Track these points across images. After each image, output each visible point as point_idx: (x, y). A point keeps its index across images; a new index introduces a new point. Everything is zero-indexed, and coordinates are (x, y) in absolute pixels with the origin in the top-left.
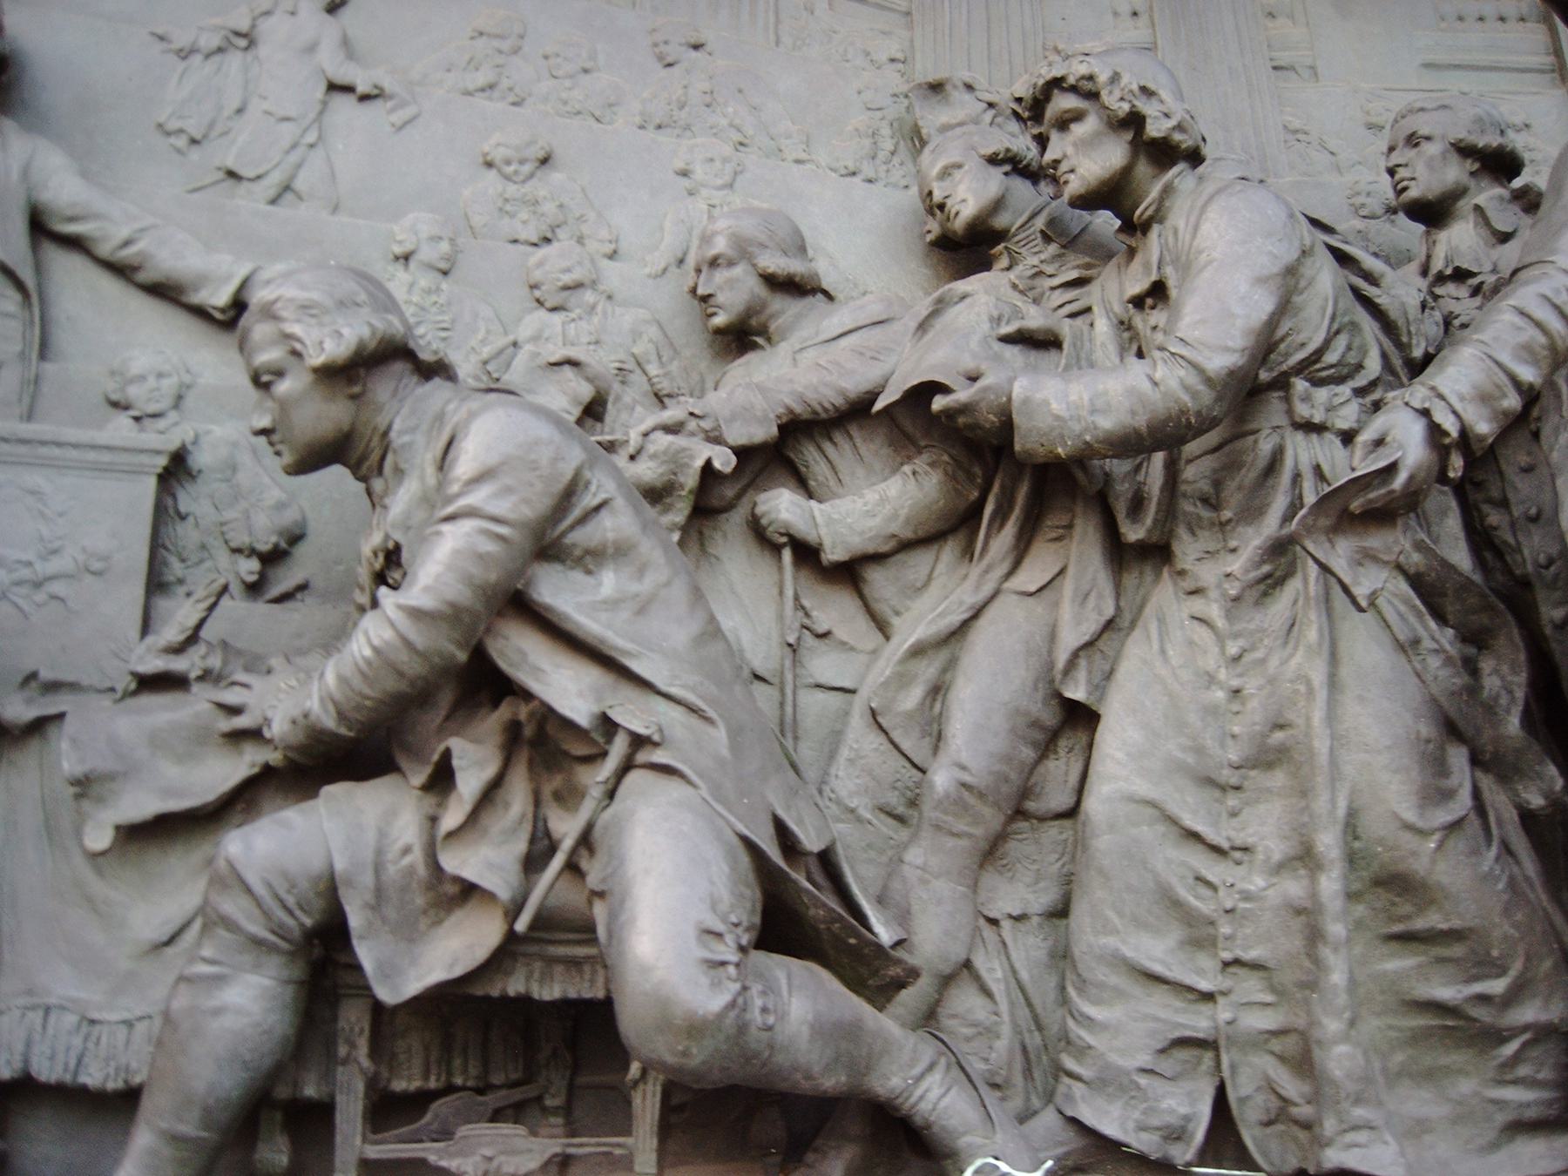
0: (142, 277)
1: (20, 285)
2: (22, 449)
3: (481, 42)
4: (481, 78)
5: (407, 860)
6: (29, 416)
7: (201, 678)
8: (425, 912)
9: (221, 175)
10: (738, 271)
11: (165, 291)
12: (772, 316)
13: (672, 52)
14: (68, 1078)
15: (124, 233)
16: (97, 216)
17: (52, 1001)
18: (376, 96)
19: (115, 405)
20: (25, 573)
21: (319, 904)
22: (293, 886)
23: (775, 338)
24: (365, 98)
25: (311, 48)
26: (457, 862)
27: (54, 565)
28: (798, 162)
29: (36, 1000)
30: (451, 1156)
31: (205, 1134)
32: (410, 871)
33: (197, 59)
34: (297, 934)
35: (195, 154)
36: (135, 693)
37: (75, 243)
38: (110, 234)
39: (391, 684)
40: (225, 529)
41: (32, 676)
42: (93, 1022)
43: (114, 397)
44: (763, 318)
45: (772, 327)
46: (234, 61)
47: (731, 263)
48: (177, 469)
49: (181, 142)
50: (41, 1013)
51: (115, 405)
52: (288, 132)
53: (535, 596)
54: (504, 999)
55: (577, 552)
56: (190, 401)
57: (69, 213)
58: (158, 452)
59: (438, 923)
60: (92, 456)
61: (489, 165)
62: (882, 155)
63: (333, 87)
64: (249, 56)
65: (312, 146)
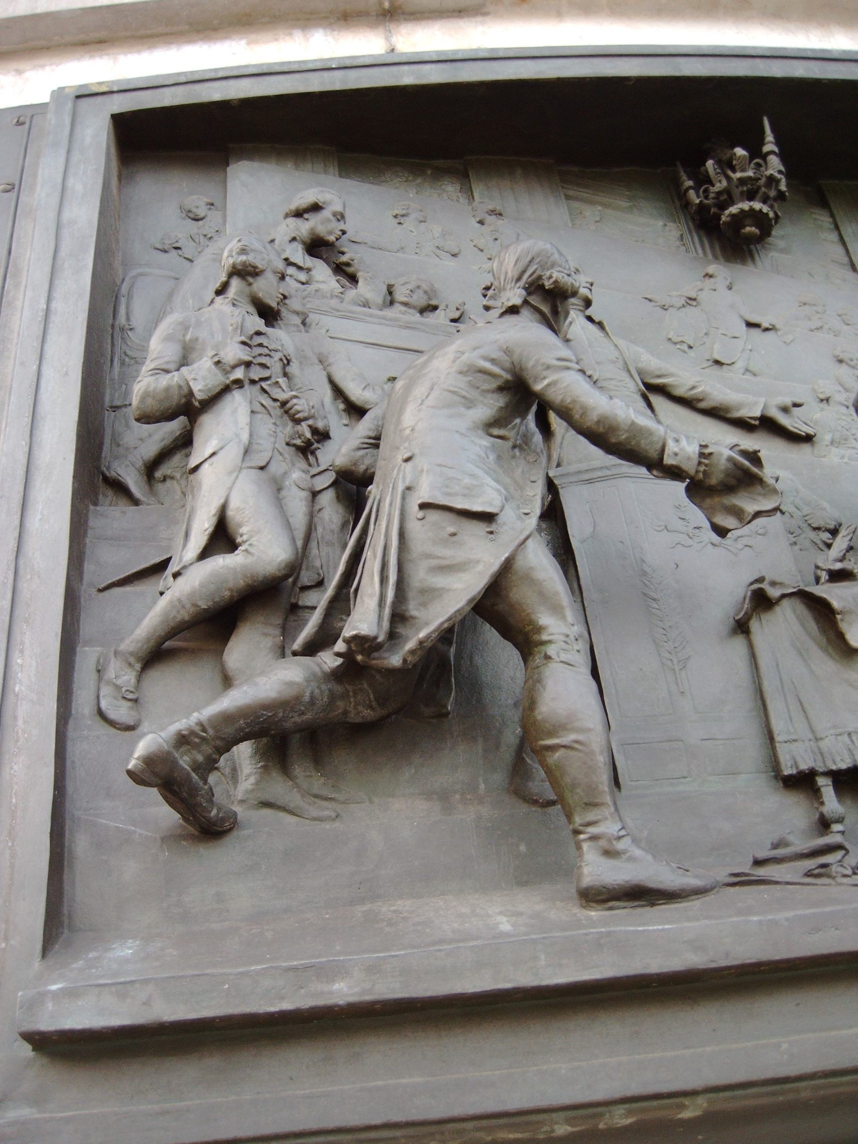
0: (702, 405)
3: (806, 307)
9: (710, 363)
15: (691, 383)
17: (850, 729)
24: (767, 329)
29: (841, 730)
35: (692, 353)
37: (662, 390)
49: (685, 347)
57: (658, 373)
61: (841, 361)
63: (750, 325)
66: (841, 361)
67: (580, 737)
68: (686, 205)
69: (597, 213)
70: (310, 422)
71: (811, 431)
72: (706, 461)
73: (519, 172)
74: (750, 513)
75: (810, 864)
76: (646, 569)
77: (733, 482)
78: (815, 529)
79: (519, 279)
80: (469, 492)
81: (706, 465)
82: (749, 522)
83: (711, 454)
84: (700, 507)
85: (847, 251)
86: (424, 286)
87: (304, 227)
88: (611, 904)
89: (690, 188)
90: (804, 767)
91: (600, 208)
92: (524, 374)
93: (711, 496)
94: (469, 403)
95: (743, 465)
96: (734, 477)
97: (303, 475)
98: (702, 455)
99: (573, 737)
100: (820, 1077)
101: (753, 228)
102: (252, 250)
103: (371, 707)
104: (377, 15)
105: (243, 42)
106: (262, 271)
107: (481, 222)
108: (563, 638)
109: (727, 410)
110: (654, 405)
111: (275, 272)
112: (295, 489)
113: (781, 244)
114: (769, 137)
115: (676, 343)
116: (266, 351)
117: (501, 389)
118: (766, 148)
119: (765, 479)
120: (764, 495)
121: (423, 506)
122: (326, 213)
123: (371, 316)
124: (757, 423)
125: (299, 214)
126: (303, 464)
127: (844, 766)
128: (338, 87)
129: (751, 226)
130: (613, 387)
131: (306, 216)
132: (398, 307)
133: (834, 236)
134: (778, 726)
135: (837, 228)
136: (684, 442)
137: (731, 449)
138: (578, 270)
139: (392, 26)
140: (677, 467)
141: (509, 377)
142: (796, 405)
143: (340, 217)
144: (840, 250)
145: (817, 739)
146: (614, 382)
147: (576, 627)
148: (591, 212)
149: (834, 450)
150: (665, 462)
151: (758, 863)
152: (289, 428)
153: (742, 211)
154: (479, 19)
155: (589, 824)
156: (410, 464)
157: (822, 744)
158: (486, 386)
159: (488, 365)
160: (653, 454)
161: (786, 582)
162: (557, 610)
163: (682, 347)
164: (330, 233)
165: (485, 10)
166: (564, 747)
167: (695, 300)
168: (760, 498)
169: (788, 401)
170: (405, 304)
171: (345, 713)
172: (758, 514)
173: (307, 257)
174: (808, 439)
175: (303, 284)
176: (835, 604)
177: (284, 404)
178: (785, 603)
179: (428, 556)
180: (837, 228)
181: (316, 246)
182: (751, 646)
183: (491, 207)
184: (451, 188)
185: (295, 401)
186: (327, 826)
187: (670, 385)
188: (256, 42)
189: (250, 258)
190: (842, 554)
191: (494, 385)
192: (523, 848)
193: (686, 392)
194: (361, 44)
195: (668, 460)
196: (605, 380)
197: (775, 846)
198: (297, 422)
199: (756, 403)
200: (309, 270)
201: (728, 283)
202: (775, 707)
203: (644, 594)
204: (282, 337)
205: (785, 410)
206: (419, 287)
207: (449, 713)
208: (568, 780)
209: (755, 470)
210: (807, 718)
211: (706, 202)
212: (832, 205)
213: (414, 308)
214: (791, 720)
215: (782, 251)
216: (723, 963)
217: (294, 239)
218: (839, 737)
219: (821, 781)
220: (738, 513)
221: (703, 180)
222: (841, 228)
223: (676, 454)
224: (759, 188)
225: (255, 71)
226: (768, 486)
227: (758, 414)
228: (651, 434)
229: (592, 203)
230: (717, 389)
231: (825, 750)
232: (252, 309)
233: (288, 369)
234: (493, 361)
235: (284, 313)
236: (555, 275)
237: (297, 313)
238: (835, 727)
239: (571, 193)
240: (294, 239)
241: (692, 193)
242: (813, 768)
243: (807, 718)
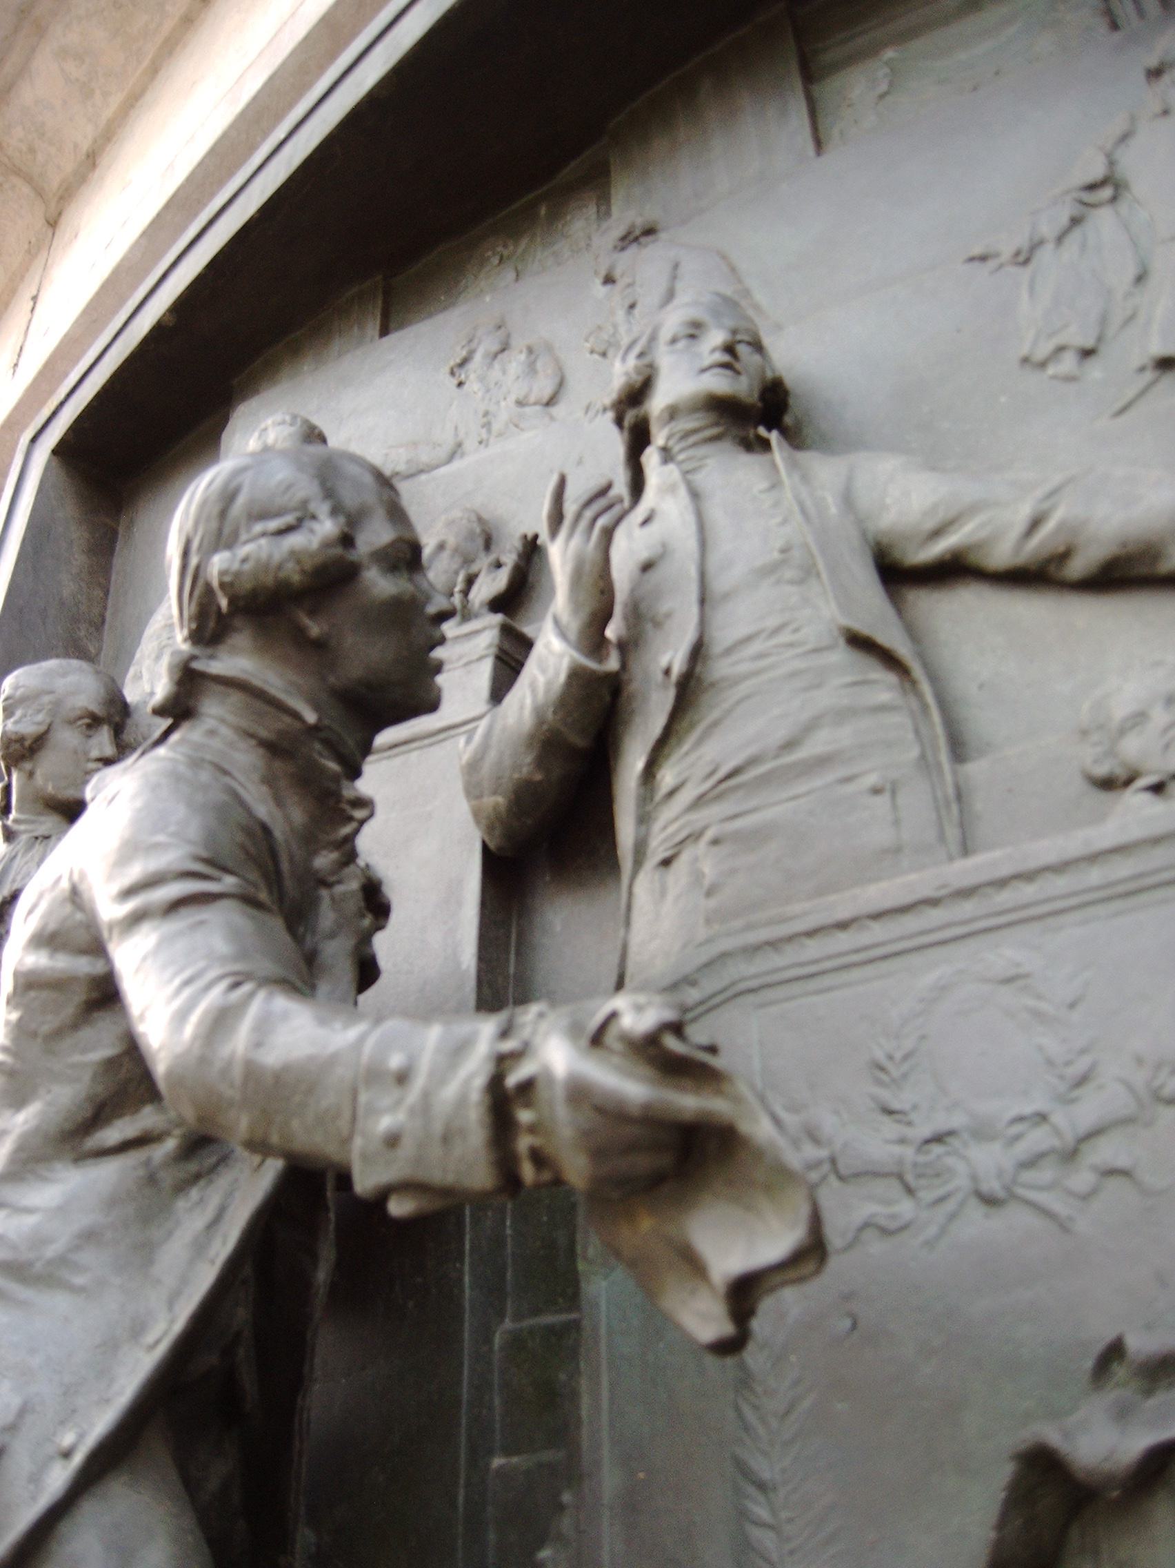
0: (1077, 567)
1: (889, 659)
2: (968, 908)
6: (966, 850)
9: (1149, 375)
15: (1024, 512)
16: (973, 509)
19: (1108, 784)
20: (1038, 1139)
27: (1088, 1111)
33: (1046, 255)
35: (1095, 371)
37: (954, 570)
41: (1114, 1352)
43: (1101, 770)
46: (1104, 222)
49: (1068, 363)
51: (1108, 784)
57: (930, 524)
60: (1095, 875)
64: (1123, 207)
77: (643, 1163)
107: (609, 280)
111: (71, 722)
120: (769, 1189)
130: (743, 668)
167: (1103, 183)
187: (969, 548)
191: (69, 1010)
209: (688, 1102)
223: (392, 1140)
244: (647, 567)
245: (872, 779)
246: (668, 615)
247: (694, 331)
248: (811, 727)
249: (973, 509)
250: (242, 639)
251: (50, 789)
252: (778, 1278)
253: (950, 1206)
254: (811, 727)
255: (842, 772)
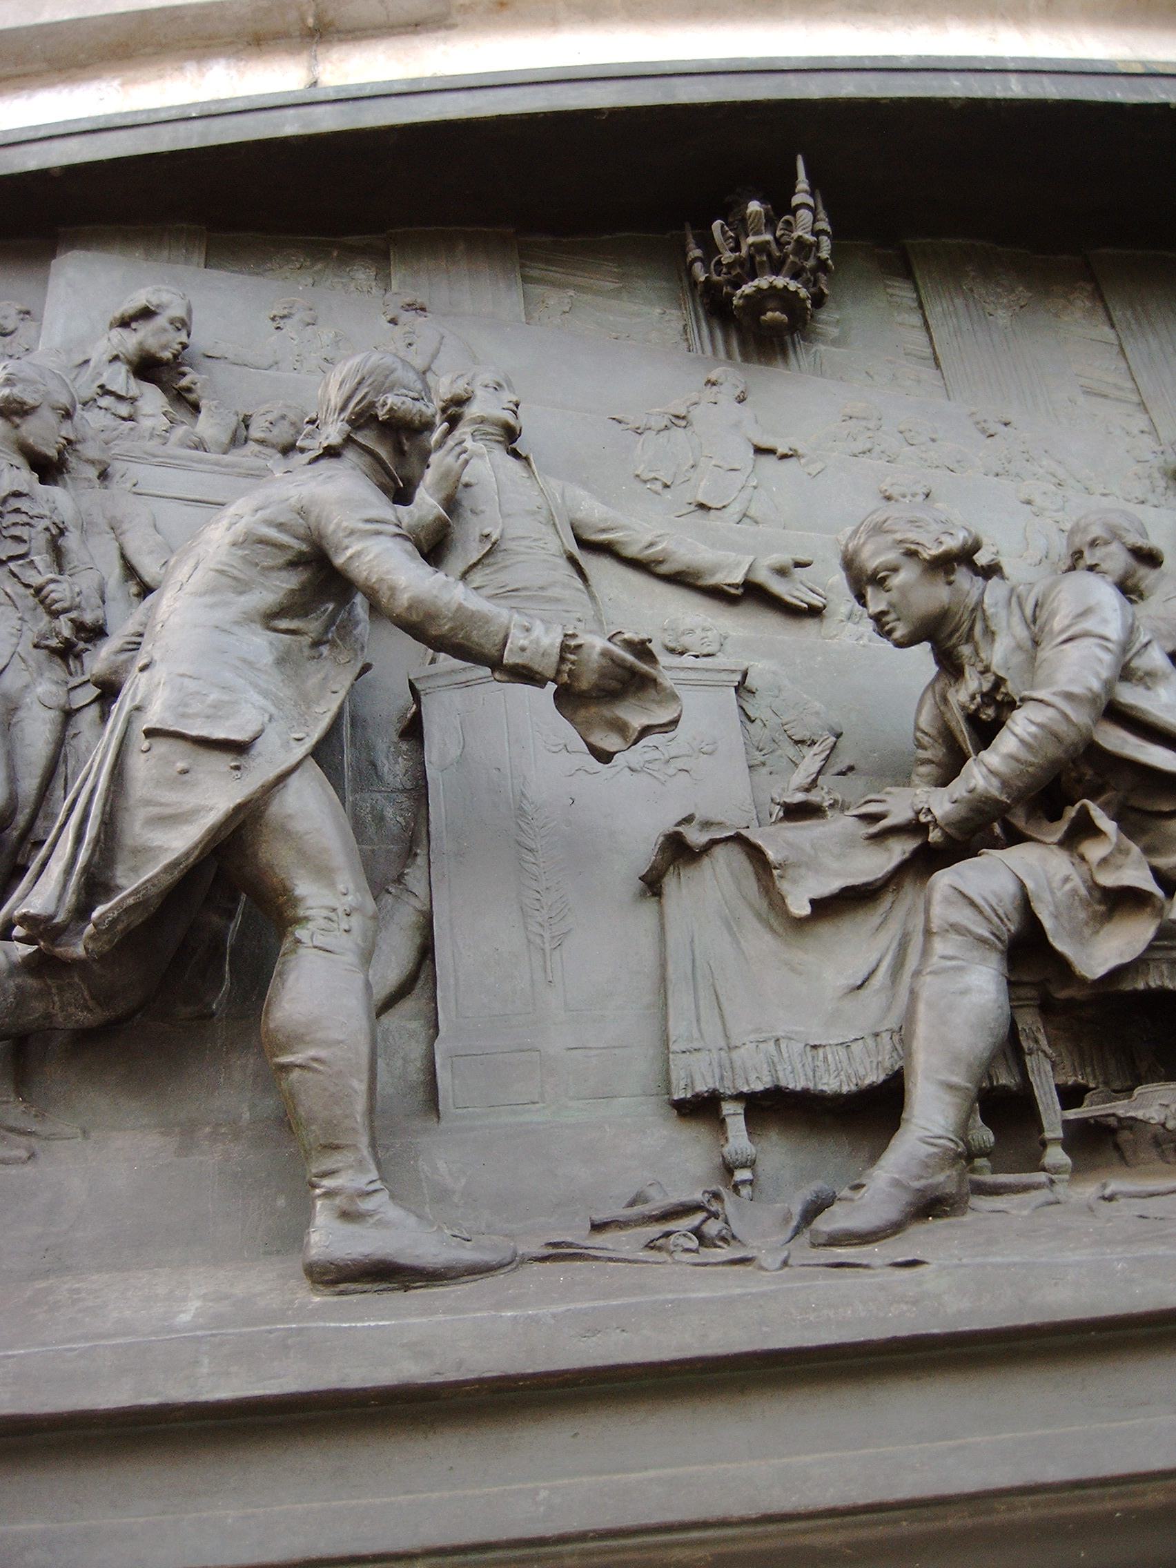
0: (663, 569)
3: (850, 423)
4: (862, 444)
5: (1068, 887)
7: (831, 806)
8: (1087, 924)
9: (692, 507)
10: (1115, 547)
11: (683, 580)
12: (1140, 579)
13: (993, 427)
14: (811, 1086)
15: (648, 538)
16: (623, 528)
17: (780, 1034)
18: (791, 456)
19: (672, 651)
21: (1016, 917)
22: (1001, 901)
23: (1146, 594)
24: (784, 457)
25: (737, 425)
26: (1108, 879)
28: (1104, 495)
29: (764, 1035)
30: (1136, 1109)
31: (969, 1085)
32: (1074, 892)
34: (1005, 937)
35: (668, 495)
36: (781, 820)
37: (606, 549)
38: (635, 543)
39: (1053, 751)
40: (786, 727)
42: (815, 1047)
43: (672, 645)
44: (1135, 580)
45: (1143, 586)
46: (678, 434)
47: (1107, 543)
48: (742, 688)
49: (658, 486)
50: (772, 1043)
52: (739, 478)
53: (1121, 700)
54: (1149, 992)
55: (1140, 673)
56: (728, 647)
57: (602, 526)
58: (733, 671)
59: (1097, 932)
61: (888, 498)
62: (1160, 490)
63: (759, 451)
65: (755, 488)
66: (888, 498)
67: (322, 1053)
68: (694, 284)
69: (567, 300)
70: (73, 615)
71: (817, 601)
72: (572, 657)
73: (462, 247)
74: (635, 729)
75: (655, 1230)
76: (527, 807)
77: (614, 684)
78: (797, 742)
79: (343, 409)
80: (216, 712)
81: (573, 663)
82: (635, 743)
83: (579, 647)
84: (571, 721)
85: (931, 339)
86: (292, 416)
87: (130, 341)
88: (342, 1286)
89: (696, 259)
90: (702, 1087)
91: (571, 293)
92: (324, 542)
93: (586, 706)
94: (242, 586)
95: (624, 660)
96: (614, 678)
97: (54, 688)
98: (564, 648)
99: (312, 1052)
100: (593, 1539)
101: (777, 314)
102: (23, 380)
103: (86, 1008)
104: (302, 36)
105: (116, 83)
106: (34, 409)
107: (393, 321)
108: (325, 913)
109: (698, 574)
110: (587, 571)
111: (54, 409)
112: (38, 710)
113: (834, 332)
114: (803, 183)
115: (645, 482)
116: (25, 519)
117: (292, 564)
118: (796, 200)
119: (660, 680)
120: (659, 703)
121: (150, 733)
122: (161, 321)
123: (200, 461)
124: (739, 592)
125: (125, 323)
126: (58, 672)
127: (759, 1087)
128: (194, 143)
129: (773, 310)
130: (522, 549)
131: (134, 325)
132: (252, 447)
133: (916, 320)
134: (679, 1028)
135: (921, 306)
136: (538, 629)
137: (609, 640)
138: (499, 385)
139: (321, 50)
140: (524, 667)
141: (304, 547)
142: (798, 565)
143: (182, 324)
144: (922, 337)
145: (731, 1048)
146: (526, 542)
147: (350, 898)
148: (556, 299)
149: (850, 624)
150: (505, 661)
151: (597, 1227)
152: (44, 622)
153: (759, 290)
154: (442, 34)
155: (325, 1175)
156: (145, 674)
157: (735, 1055)
158: (269, 562)
159: (273, 533)
160: (490, 649)
161: (729, 823)
162: (323, 873)
163: (653, 487)
164: (165, 347)
165: (448, 22)
166: (299, 1066)
167: (684, 418)
168: (654, 707)
169: (785, 558)
170: (261, 442)
171: (48, 1016)
172: (646, 731)
173: (132, 381)
174: (814, 612)
175: (124, 419)
176: (771, 855)
177: (38, 591)
178: (719, 851)
179: (148, 803)
180: (921, 306)
181: (147, 368)
182: (661, 915)
183: (408, 300)
184: (363, 275)
185: (52, 586)
186: (13, 1171)
187: (618, 542)
188: (134, 81)
189: (17, 391)
190: (809, 780)
191: (281, 560)
192: (281, 1202)
193: (641, 550)
194: (273, 78)
195: (508, 659)
196: (513, 539)
197: (632, 1204)
198: (55, 615)
199: (738, 564)
200: (133, 400)
201: (738, 392)
202: (680, 1000)
203: (519, 843)
204: (57, 500)
205: (782, 572)
206: (283, 417)
207: (213, 1014)
208: (302, 1112)
209: (644, 667)
210: (722, 1017)
211: (715, 278)
212: (917, 274)
213: (273, 446)
214: (698, 1021)
215: (835, 342)
216: (452, 1376)
217: (116, 358)
218: (761, 1045)
219: (728, 1108)
220: (620, 727)
221: (710, 248)
222: (927, 307)
223: (523, 649)
224: (786, 256)
225: (88, 127)
226: (665, 689)
227: (738, 578)
228: (487, 622)
229: (562, 286)
230: (687, 546)
231: (738, 1064)
232: (19, 460)
233: (60, 541)
234: (280, 526)
235: (72, 462)
236: (391, 400)
237: (92, 462)
238: (758, 1030)
239: (535, 273)
240: (116, 358)
241: (698, 267)
242: (715, 1090)
243: (722, 1017)
244: (467, 485)
245: (578, 615)
246: (483, 512)
247: (498, 387)
248: (553, 584)
249: (623, 528)
250: (366, 432)
251: (31, 441)
252: (657, 730)
253: (618, 769)
254: (553, 584)
255: (565, 608)
